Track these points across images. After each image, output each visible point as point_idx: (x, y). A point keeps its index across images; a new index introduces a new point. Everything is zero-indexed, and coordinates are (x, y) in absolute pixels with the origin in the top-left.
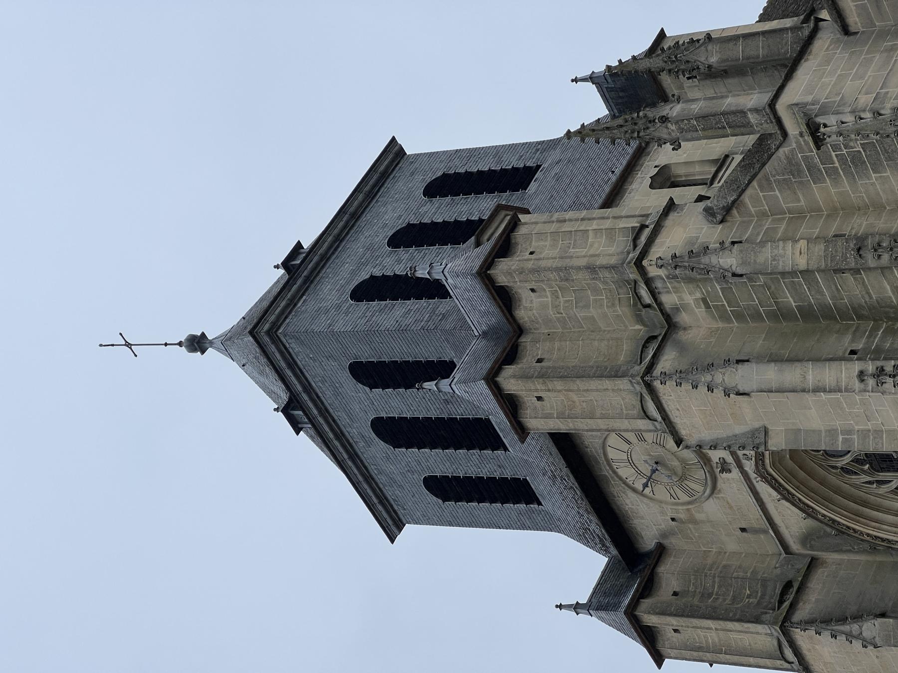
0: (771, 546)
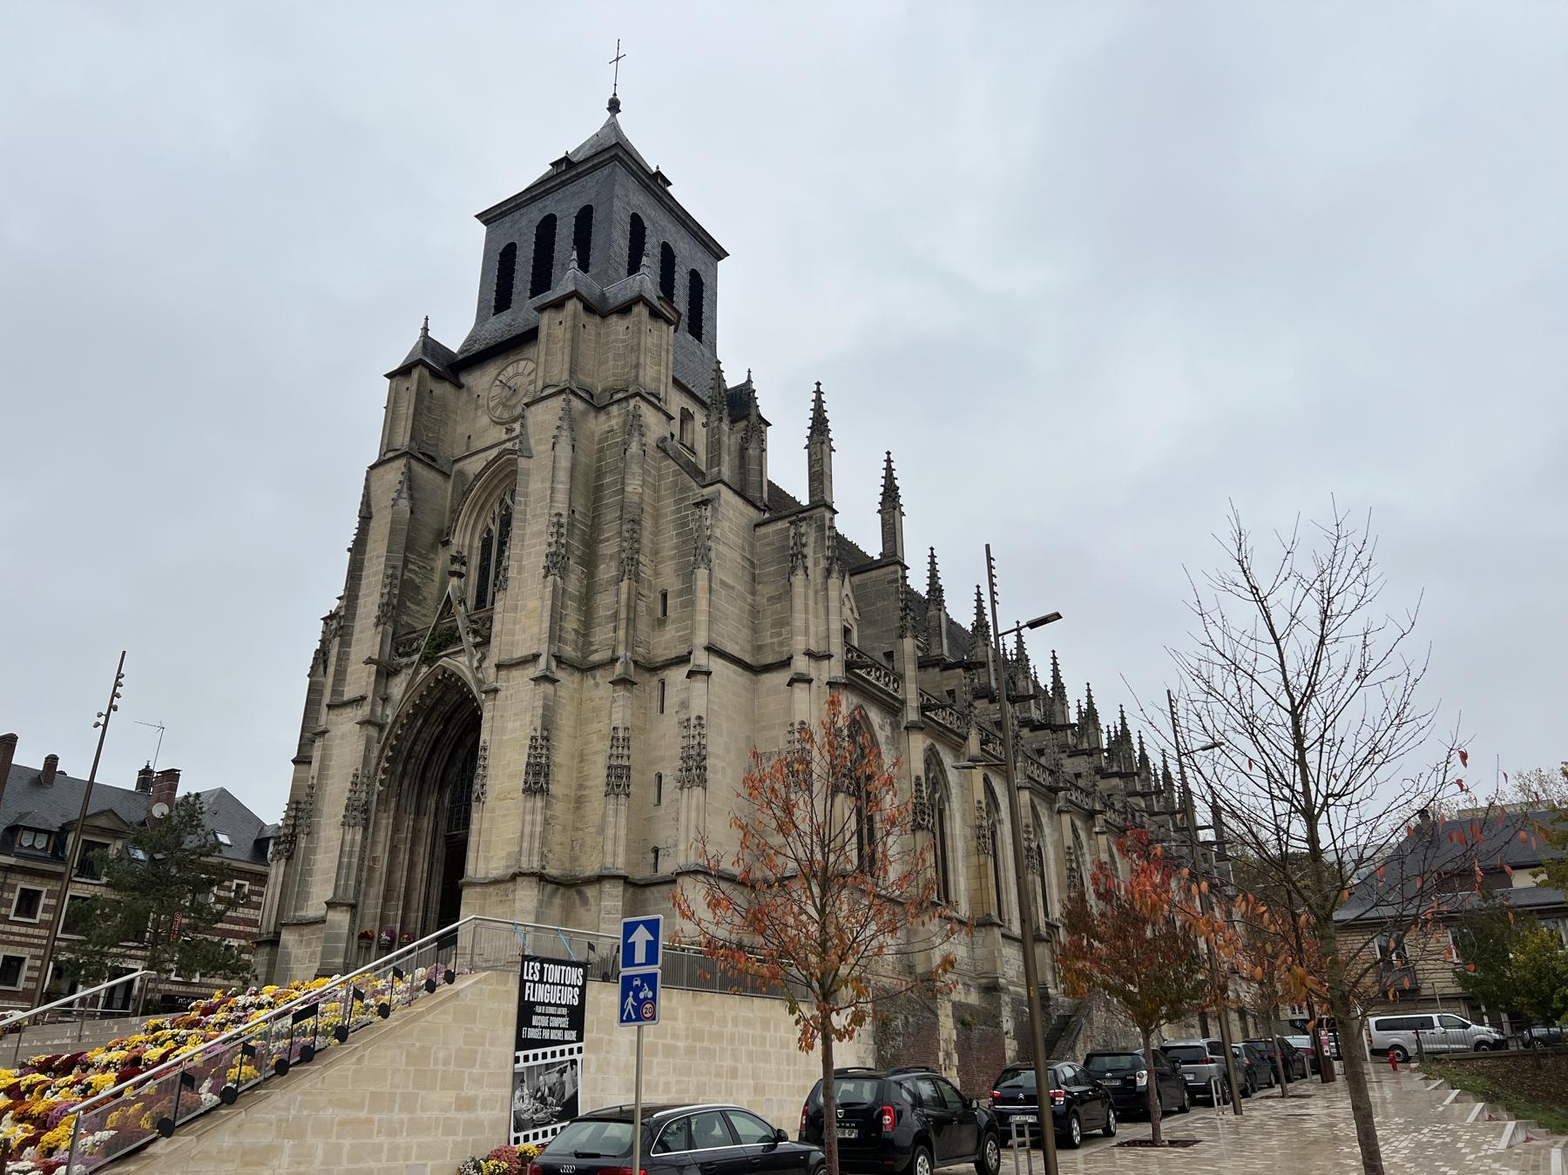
0: (458, 453)
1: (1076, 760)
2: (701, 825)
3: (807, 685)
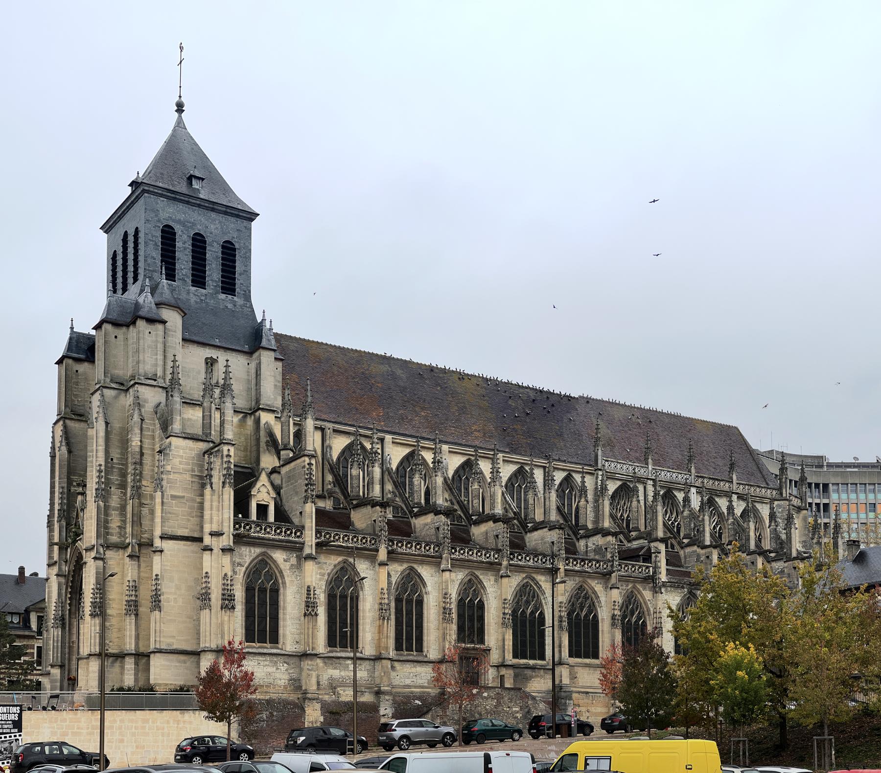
1: (551, 532)
2: (158, 629)
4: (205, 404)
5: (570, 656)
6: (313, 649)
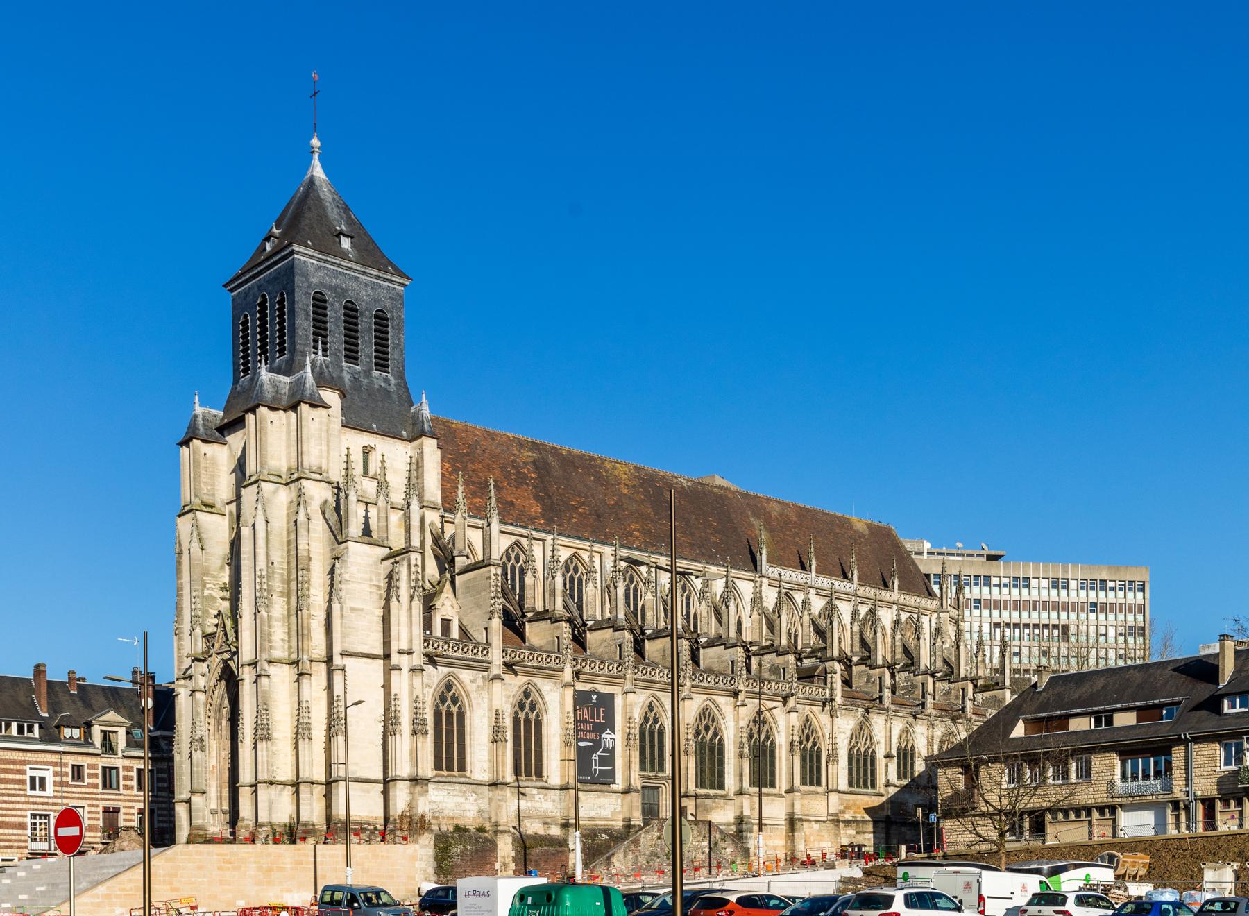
3: (397, 672)
4: (380, 504)
5: (803, 782)
6: (503, 777)
